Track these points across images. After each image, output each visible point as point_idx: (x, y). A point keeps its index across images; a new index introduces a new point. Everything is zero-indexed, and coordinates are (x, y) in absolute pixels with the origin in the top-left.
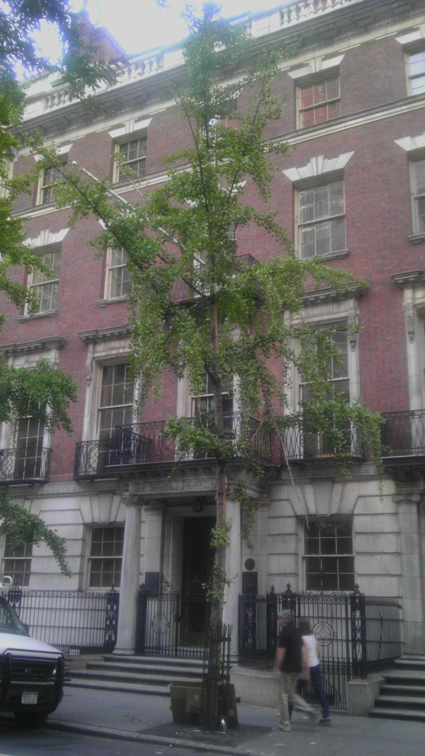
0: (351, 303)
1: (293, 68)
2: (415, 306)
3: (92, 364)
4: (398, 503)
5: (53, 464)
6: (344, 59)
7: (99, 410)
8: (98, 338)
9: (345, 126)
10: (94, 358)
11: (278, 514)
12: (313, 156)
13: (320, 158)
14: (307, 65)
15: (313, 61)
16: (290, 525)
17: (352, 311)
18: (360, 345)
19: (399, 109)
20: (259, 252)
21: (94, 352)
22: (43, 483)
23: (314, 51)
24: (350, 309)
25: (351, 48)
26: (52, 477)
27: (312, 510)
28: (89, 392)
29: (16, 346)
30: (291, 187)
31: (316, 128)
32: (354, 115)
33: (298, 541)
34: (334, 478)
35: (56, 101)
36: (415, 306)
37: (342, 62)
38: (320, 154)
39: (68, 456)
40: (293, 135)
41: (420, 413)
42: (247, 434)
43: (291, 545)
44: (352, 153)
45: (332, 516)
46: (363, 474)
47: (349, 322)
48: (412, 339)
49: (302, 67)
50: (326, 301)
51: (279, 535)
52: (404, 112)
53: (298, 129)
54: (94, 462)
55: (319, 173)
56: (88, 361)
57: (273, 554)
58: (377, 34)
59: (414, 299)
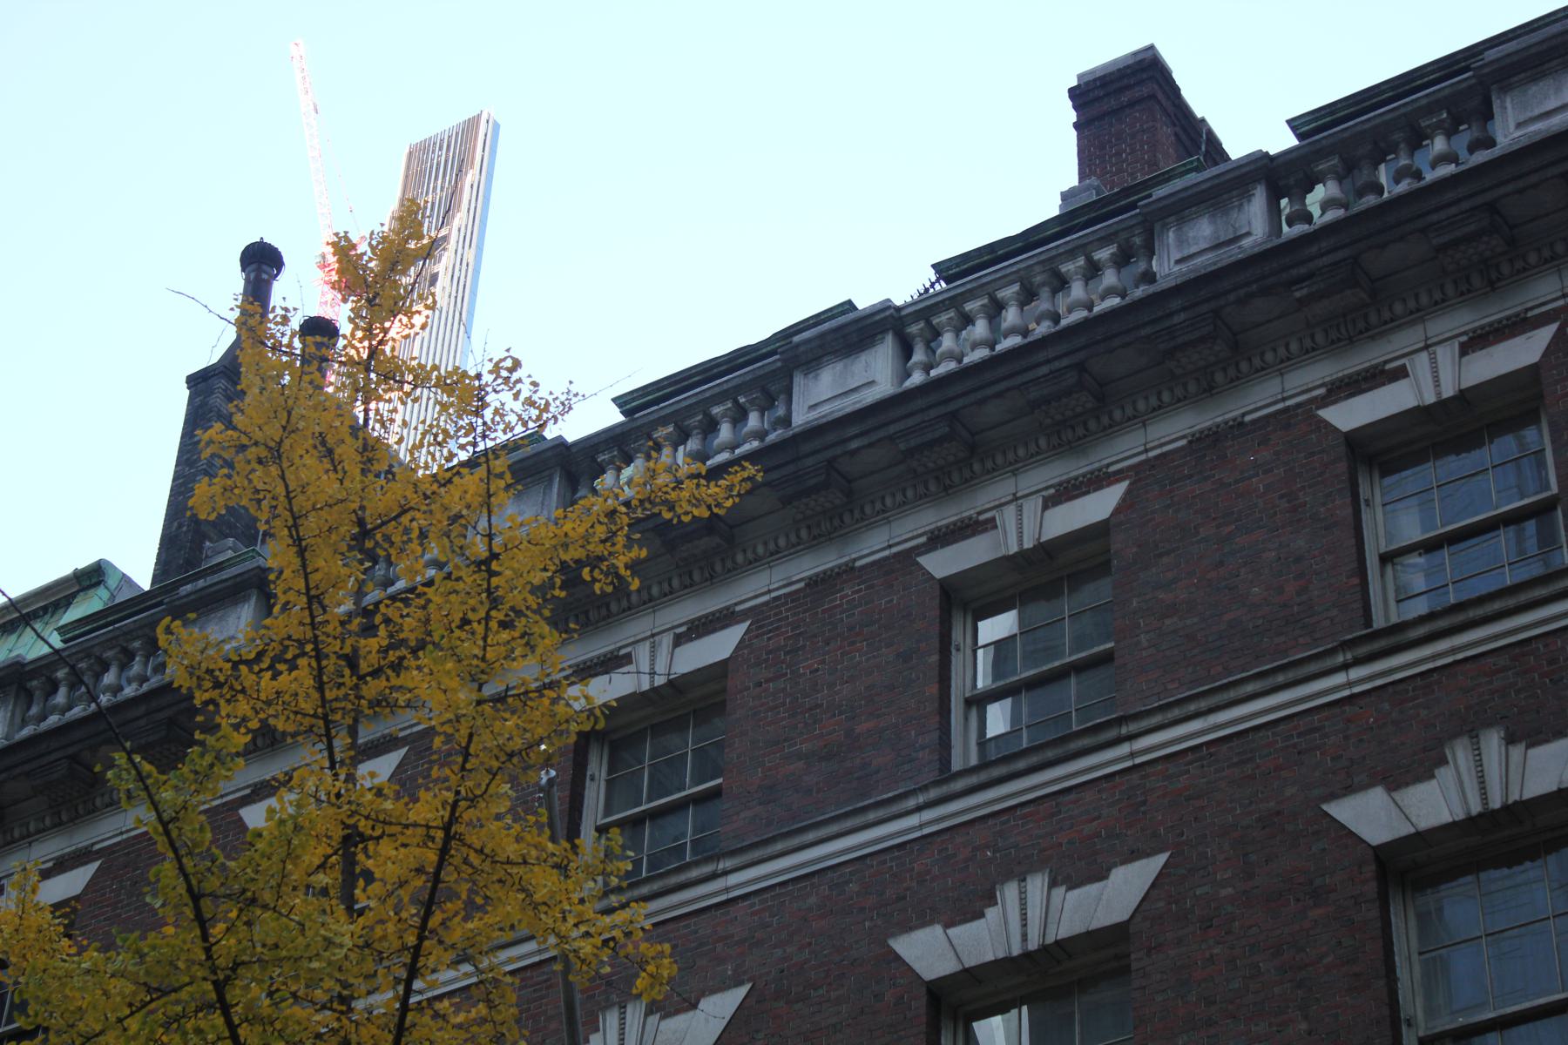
1: (940, 539)
6: (1128, 492)
9: (1132, 755)
12: (1007, 877)
13: (1037, 885)
14: (991, 524)
15: (1011, 509)
19: (1340, 678)
23: (1015, 473)
25: (1152, 454)
30: (920, 1004)
31: (1021, 765)
32: (1161, 709)
35: (61, 697)
37: (1117, 511)
38: (1033, 869)
40: (933, 793)
44: (1161, 859)
49: (973, 535)
52: (1357, 690)
53: (957, 765)
55: (1033, 945)
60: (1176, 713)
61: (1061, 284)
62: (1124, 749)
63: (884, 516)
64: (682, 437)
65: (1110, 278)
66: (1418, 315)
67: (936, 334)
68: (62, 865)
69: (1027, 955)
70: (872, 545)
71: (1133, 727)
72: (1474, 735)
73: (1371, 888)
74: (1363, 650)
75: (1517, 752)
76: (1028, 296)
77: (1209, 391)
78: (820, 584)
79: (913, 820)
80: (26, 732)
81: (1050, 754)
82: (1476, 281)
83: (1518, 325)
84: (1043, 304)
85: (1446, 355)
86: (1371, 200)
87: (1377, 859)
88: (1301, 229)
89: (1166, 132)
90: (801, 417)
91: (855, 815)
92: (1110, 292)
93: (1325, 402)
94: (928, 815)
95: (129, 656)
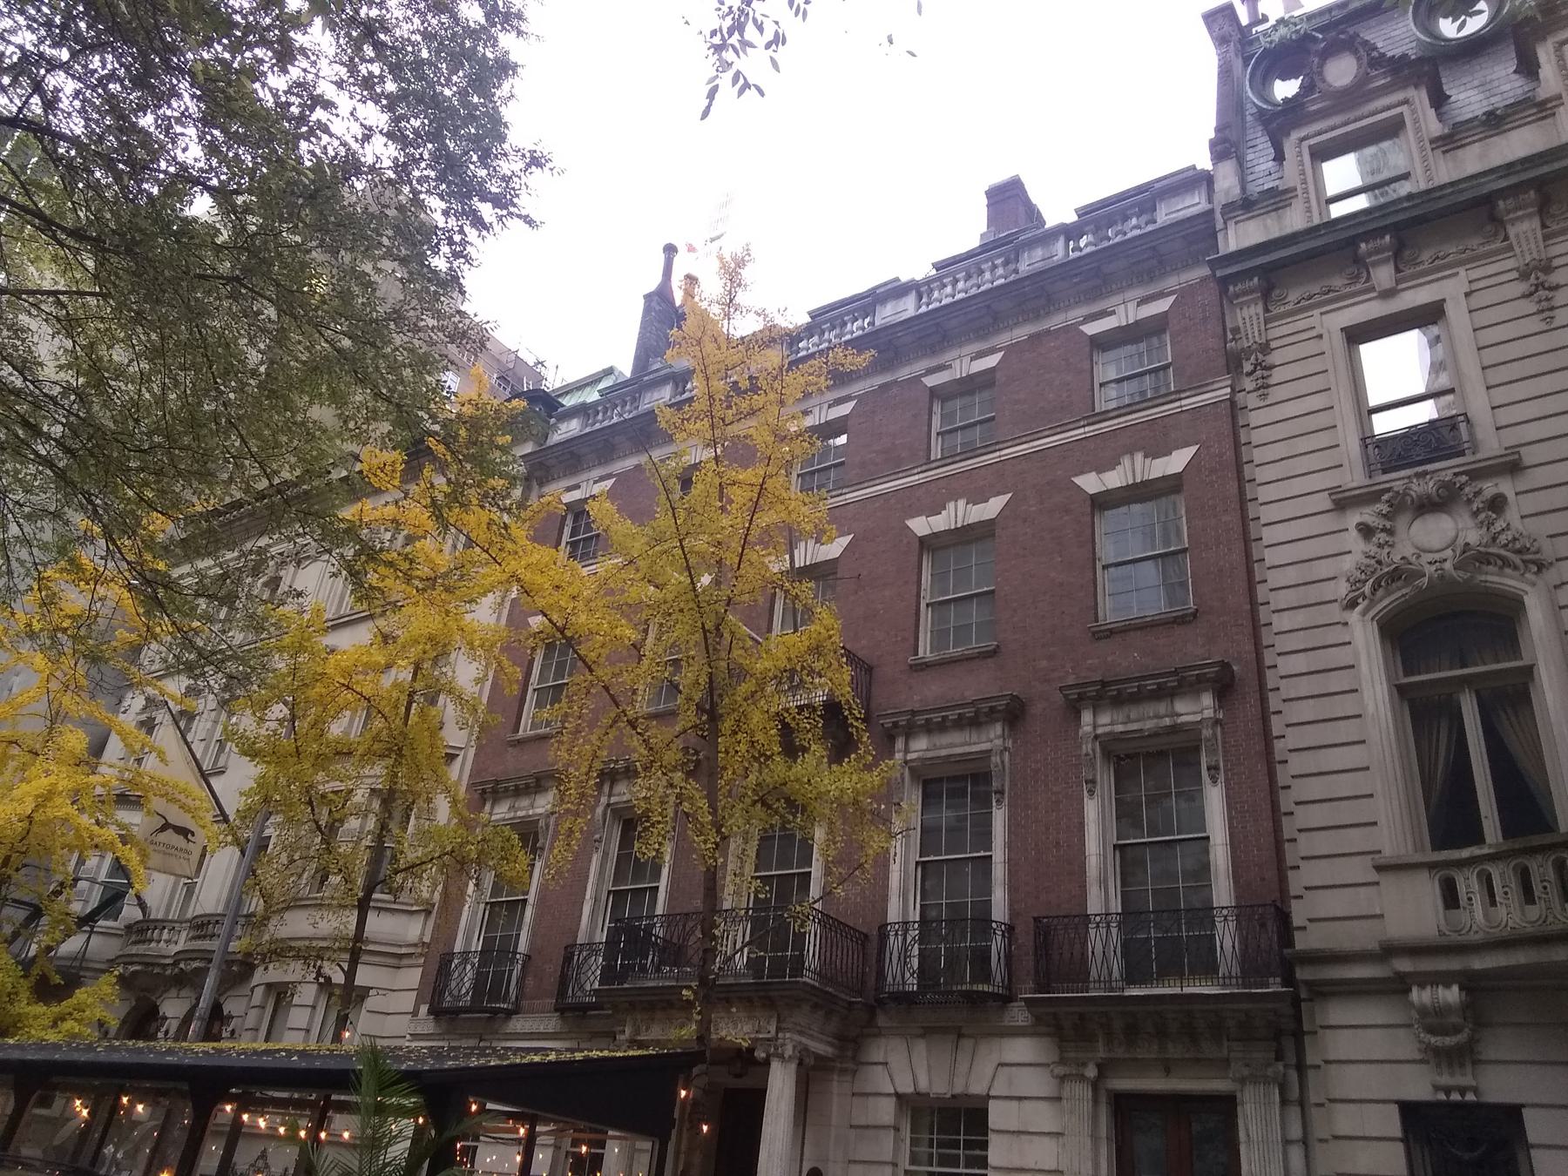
0: (998, 729)
1: (930, 371)
2: (1096, 737)
3: (605, 814)
4: (1062, 1079)
5: (530, 981)
7: (609, 892)
8: (618, 773)
10: (608, 805)
11: (868, 1090)
12: (950, 500)
13: (961, 503)
14: (950, 366)
15: (958, 361)
16: (885, 1111)
17: (999, 742)
18: (1010, 797)
19: (1082, 430)
20: (864, 642)
21: (610, 796)
22: (509, 1014)
24: (997, 737)
26: (525, 1003)
27: (923, 1085)
28: (595, 860)
29: (497, 782)
31: (958, 458)
33: (897, 1142)
34: (960, 1027)
35: (600, 417)
36: (1096, 737)
38: (961, 498)
39: (552, 969)
40: (924, 468)
41: (1098, 919)
42: (826, 944)
43: (885, 1146)
45: (954, 1096)
46: (1006, 1023)
47: (995, 759)
48: (1091, 793)
50: (960, 724)
51: (867, 1127)
54: (592, 981)
56: (599, 810)
57: (855, 1162)
58: (1056, 321)
59: (1095, 727)
60: (1018, 441)
61: (981, 272)
62: (998, 454)
63: (909, 362)
64: (833, 328)
65: (1000, 271)
66: (1121, 290)
67: (932, 291)
68: (602, 479)
69: (957, 529)
70: (904, 373)
71: (1001, 446)
72: (1132, 455)
73: (1089, 510)
74: (1091, 420)
75: (1148, 461)
76: (968, 277)
77: (1037, 316)
78: (884, 387)
79: (917, 477)
80: (588, 430)
81: (968, 455)
82: (1145, 277)
83: (1161, 295)
84: (973, 281)
85: (1131, 306)
86: (1105, 244)
87: (1092, 501)
88: (1077, 254)
89: (1021, 209)
90: (878, 323)
91: (896, 475)
92: (1001, 277)
93: (1083, 323)
94: (922, 475)
95: (625, 403)
